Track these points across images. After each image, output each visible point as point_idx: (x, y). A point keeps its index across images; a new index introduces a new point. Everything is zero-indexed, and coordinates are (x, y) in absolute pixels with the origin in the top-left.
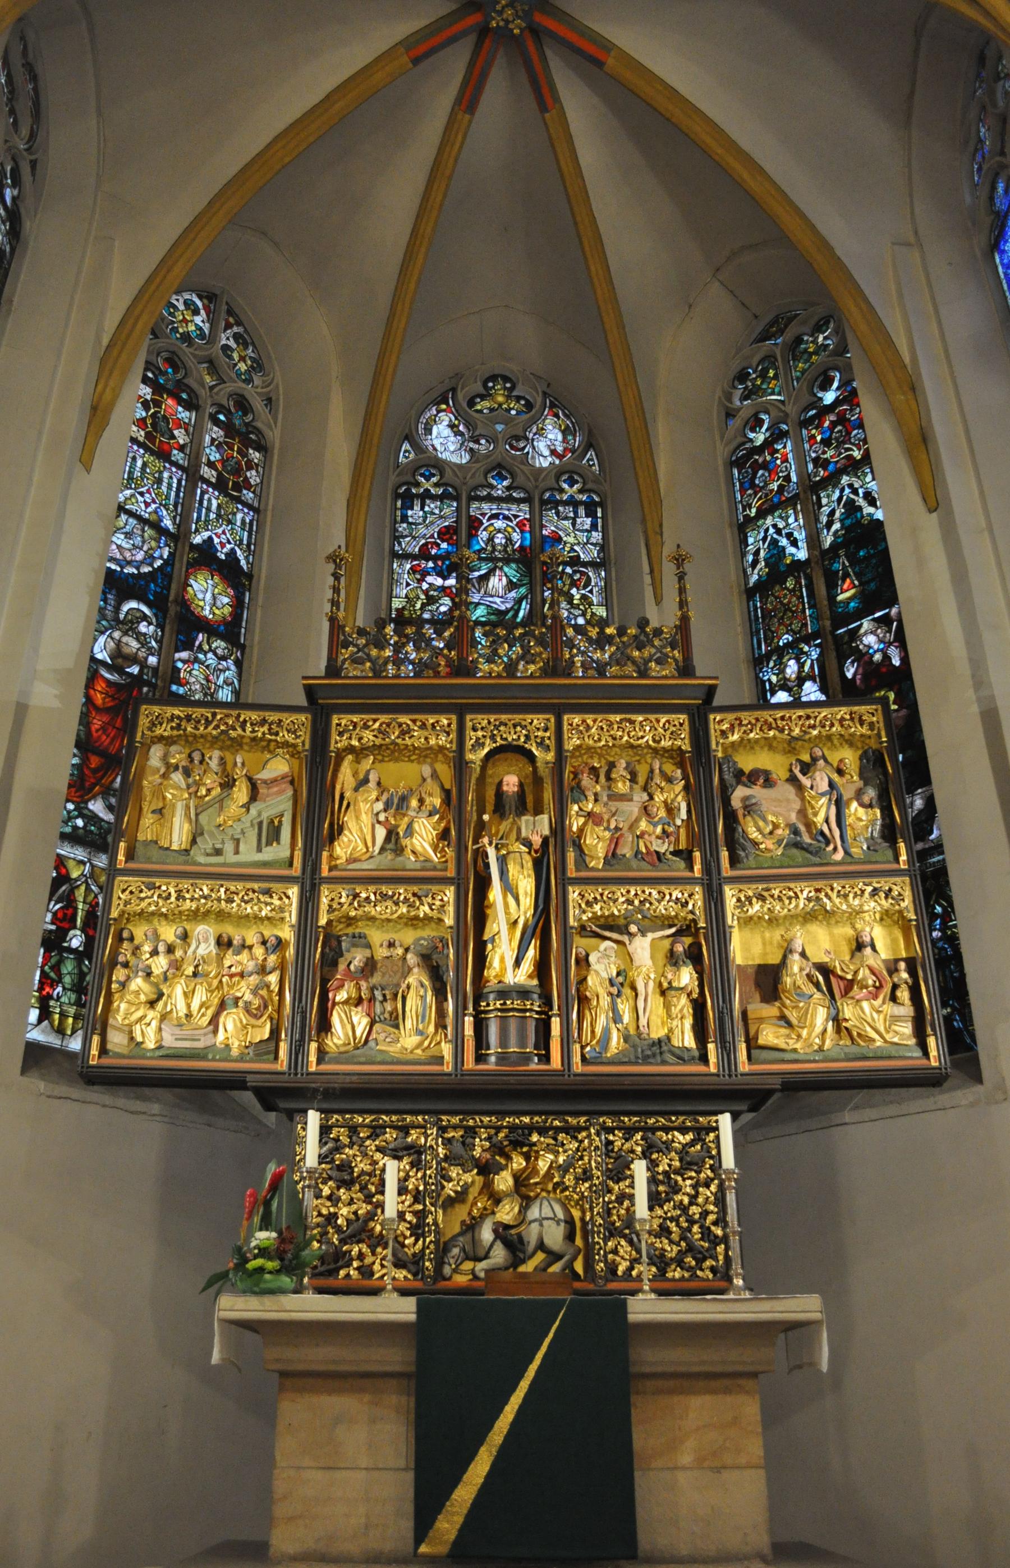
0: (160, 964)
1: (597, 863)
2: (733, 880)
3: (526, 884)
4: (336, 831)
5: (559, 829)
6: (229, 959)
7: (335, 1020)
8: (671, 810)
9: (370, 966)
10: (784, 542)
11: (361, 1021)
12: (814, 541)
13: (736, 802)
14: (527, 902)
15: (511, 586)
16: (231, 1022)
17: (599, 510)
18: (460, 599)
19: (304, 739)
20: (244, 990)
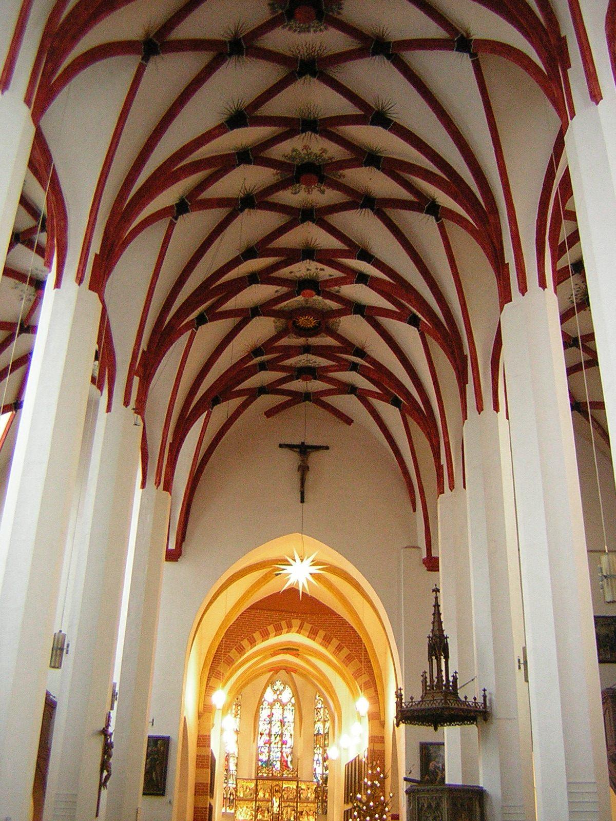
0: (241, 810)
1: (285, 799)
2: (300, 802)
3: (278, 801)
4: (258, 794)
5: (282, 795)
6: (248, 809)
7: (258, 816)
8: (294, 793)
9: (262, 810)
10: (320, 729)
11: (261, 816)
12: (324, 731)
13: (301, 792)
14: (278, 804)
15: (279, 727)
16: (248, 816)
17: (294, 711)
18: (270, 730)
19: (255, 783)
20: (249, 813)
